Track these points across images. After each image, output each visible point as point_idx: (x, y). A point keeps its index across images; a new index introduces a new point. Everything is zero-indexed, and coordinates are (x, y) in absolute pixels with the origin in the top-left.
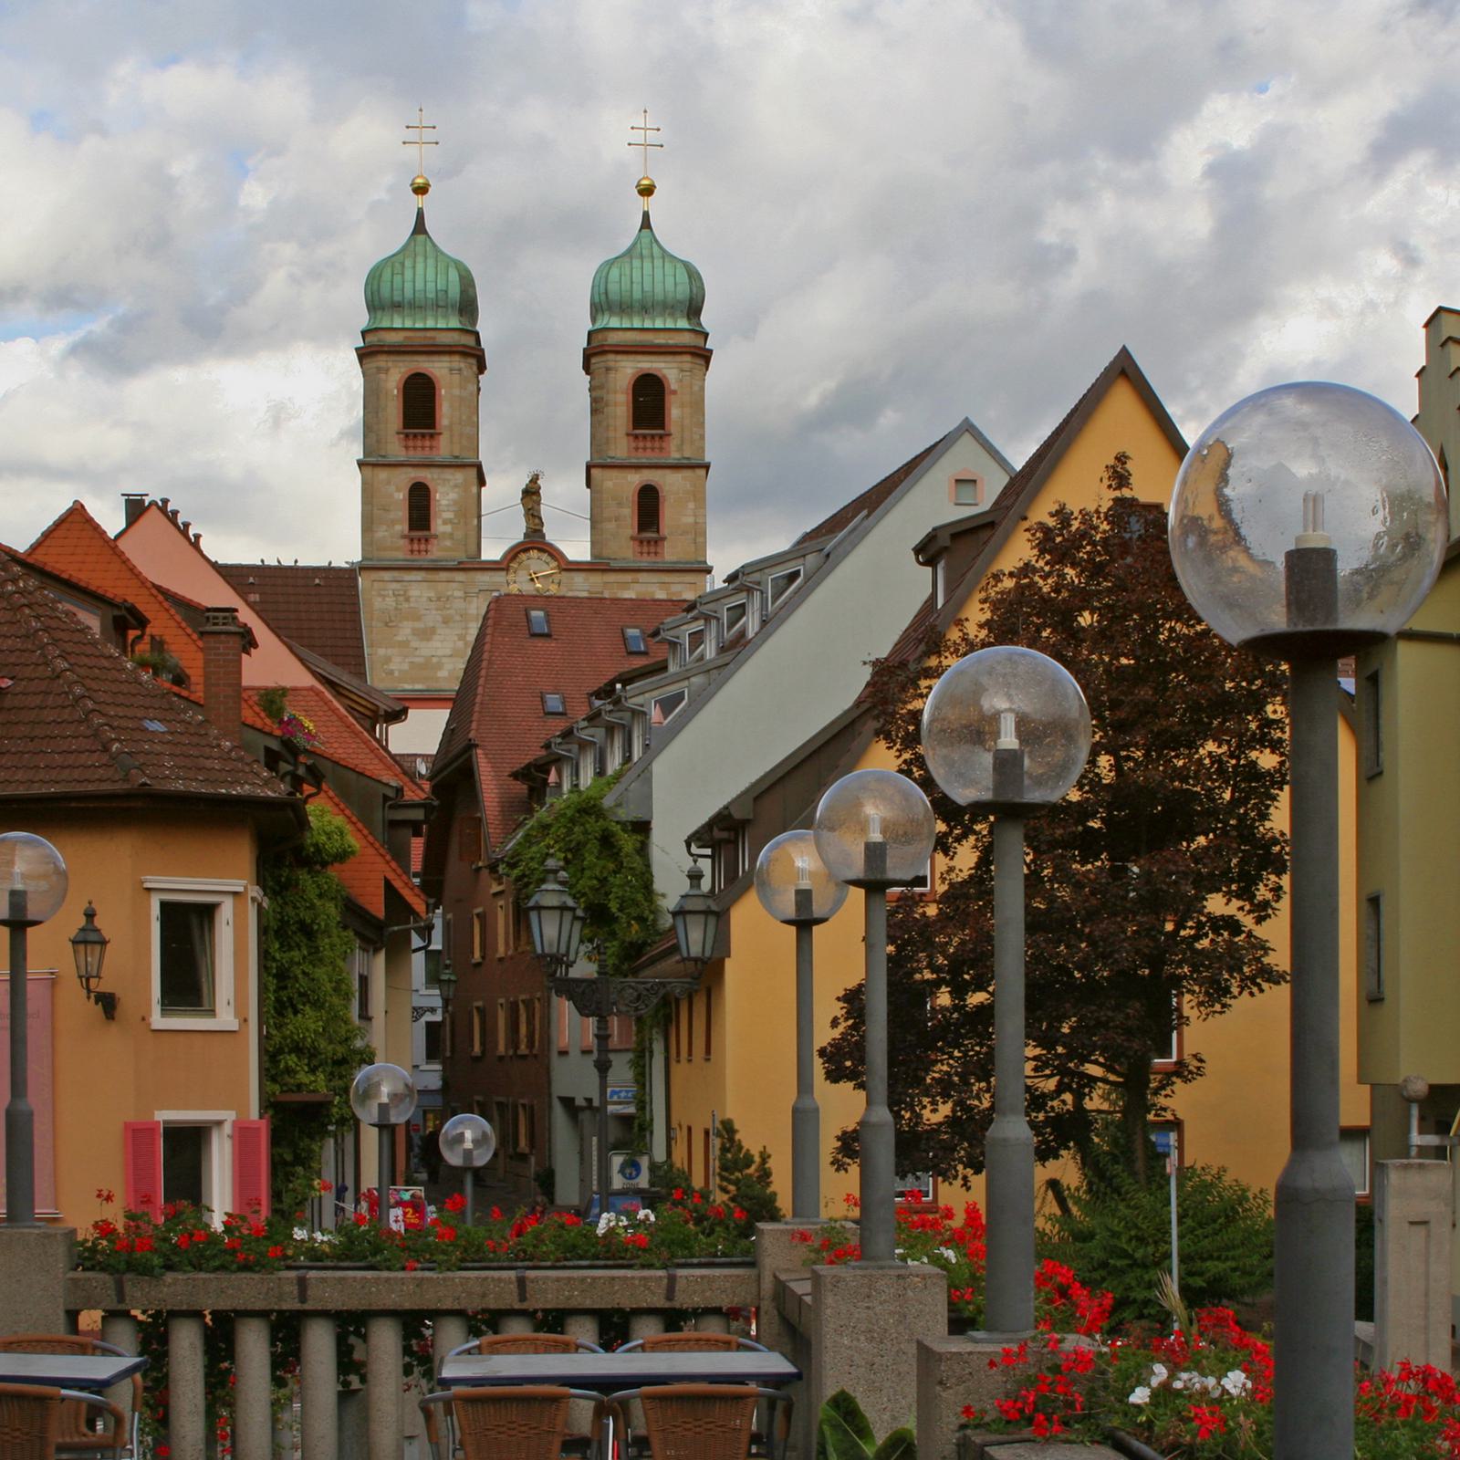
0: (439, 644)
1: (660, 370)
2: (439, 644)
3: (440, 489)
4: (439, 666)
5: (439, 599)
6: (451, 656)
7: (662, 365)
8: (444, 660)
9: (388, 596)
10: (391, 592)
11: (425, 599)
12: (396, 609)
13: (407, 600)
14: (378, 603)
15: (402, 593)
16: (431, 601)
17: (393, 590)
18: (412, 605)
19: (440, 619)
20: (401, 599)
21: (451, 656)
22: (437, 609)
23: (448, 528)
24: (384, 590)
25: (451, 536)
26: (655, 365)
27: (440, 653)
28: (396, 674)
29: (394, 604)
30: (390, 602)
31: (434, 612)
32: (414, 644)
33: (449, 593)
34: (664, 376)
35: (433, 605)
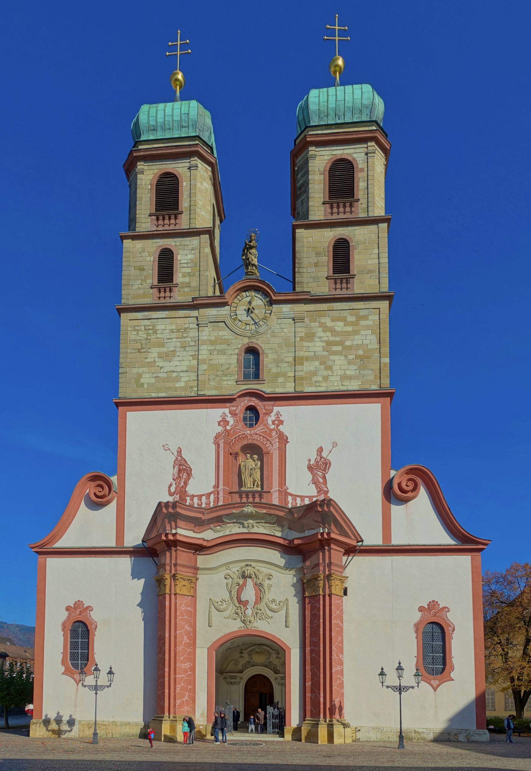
0: (178, 363)
1: (350, 155)
2: (178, 363)
3: (181, 252)
4: (178, 379)
5: (178, 331)
6: (187, 371)
7: (352, 151)
8: (182, 374)
9: (141, 330)
10: (143, 328)
11: (167, 331)
12: (147, 339)
13: (155, 332)
14: (132, 336)
15: (151, 327)
16: (173, 332)
17: (145, 326)
18: (158, 336)
19: (179, 344)
20: (150, 332)
21: (187, 371)
22: (177, 338)
23: (187, 280)
24: (138, 326)
25: (188, 285)
26: (346, 151)
27: (179, 369)
28: (146, 386)
29: (145, 336)
30: (142, 335)
31: (174, 340)
32: (160, 363)
33: (186, 326)
34: (354, 159)
35: (174, 335)
